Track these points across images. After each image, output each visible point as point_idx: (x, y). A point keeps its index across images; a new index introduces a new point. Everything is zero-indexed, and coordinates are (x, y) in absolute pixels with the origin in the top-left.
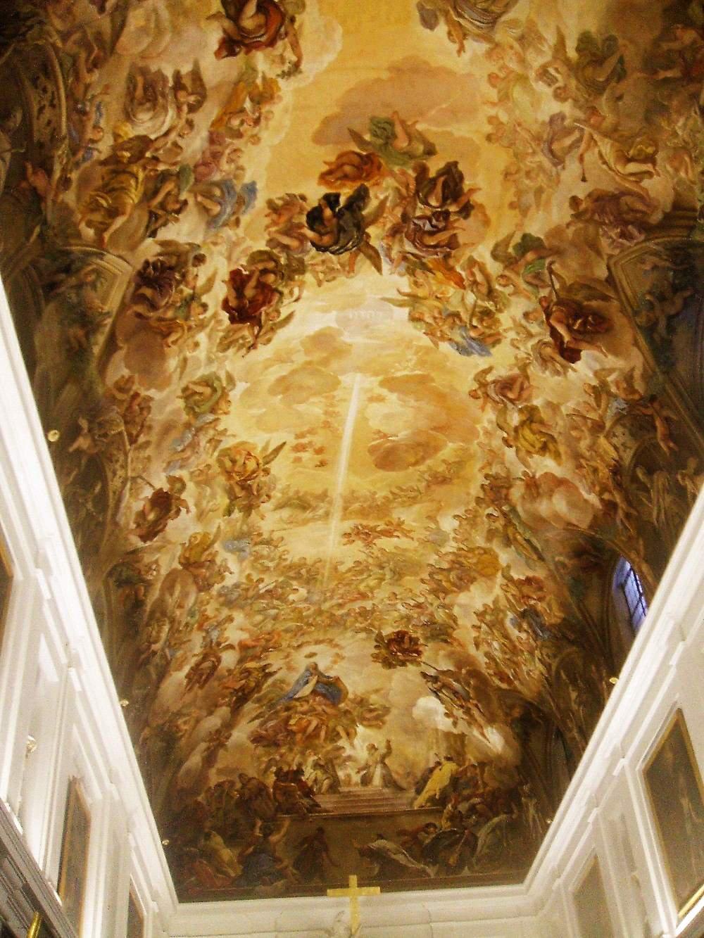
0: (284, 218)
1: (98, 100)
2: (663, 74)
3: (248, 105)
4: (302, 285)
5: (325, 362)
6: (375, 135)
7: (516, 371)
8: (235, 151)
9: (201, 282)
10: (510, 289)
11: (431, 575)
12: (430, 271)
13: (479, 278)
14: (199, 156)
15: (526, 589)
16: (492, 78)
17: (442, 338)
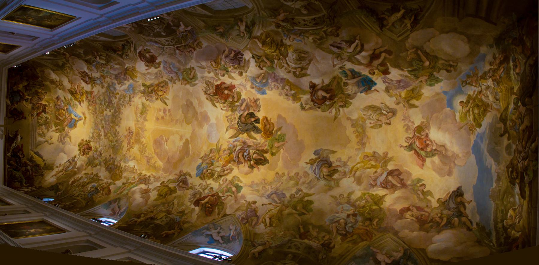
0: (252, 104)
1: (303, 40)
2: (301, 227)
3: (293, 92)
4: (227, 110)
5: (197, 119)
6: (279, 135)
7: (190, 185)
8: (278, 88)
9: (233, 74)
10: (221, 182)
11: (112, 158)
12: (229, 155)
13: (226, 172)
14: (277, 74)
15: (106, 190)
16: (297, 174)
17: (204, 160)
